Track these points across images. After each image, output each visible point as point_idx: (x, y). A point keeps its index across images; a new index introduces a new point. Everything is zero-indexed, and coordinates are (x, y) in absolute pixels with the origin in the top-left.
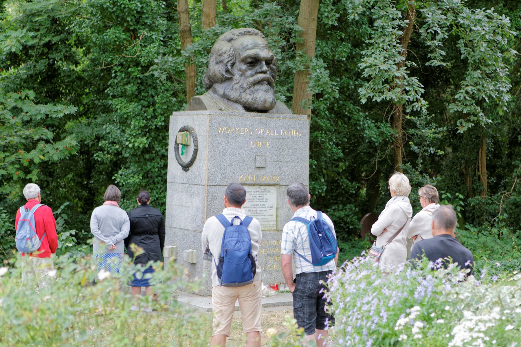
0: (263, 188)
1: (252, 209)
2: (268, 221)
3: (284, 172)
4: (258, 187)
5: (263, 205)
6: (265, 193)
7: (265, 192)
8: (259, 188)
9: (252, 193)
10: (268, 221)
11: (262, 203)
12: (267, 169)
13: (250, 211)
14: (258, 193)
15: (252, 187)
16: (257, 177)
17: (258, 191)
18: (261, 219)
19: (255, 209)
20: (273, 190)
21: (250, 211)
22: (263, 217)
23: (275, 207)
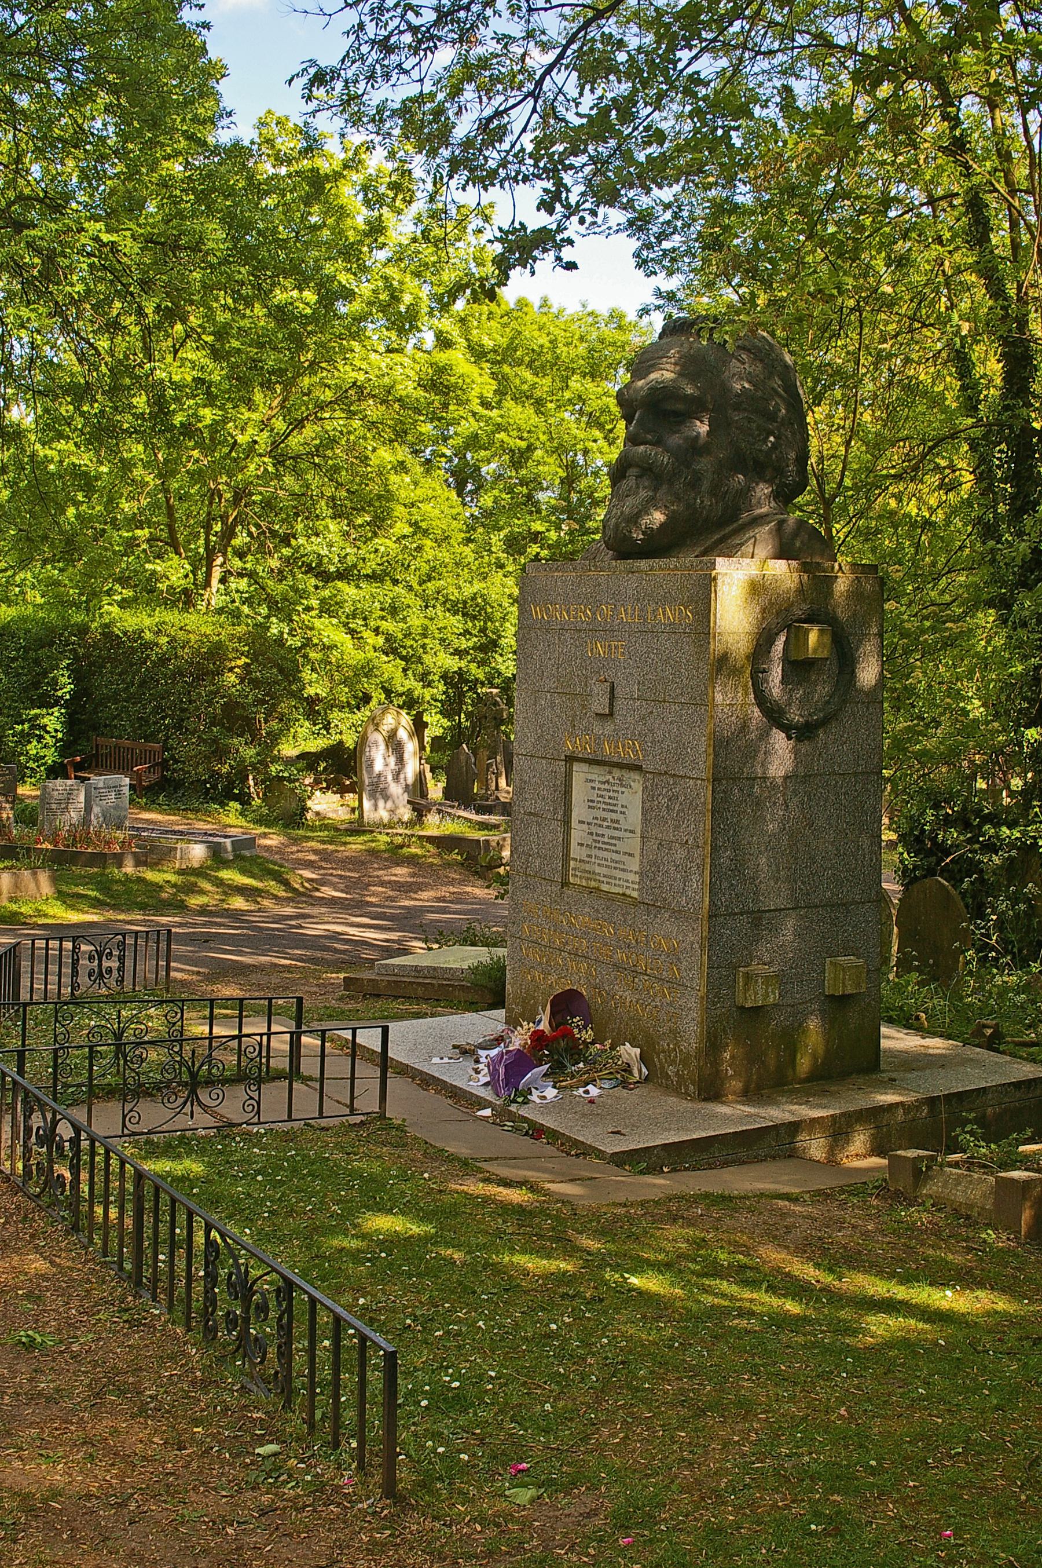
0: (617, 773)
1: (594, 829)
2: (623, 870)
3: (651, 731)
4: (607, 768)
5: (617, 822)
6: (620, 789)
7: (622, 786)
8: (610, 773)
9: (597, 785)
10: (623, 870)
11: (614, 816)
12: (618, 719)
13: (591, 834)
14: (606, 786)
15: (596, 769)
16: (598, 740)
17: (608, 782)
18: (612, 861)
19: (600, 831)
20: (636, 782)
21: (591, 834)
22: (615, 856)
23: (638, 831)
